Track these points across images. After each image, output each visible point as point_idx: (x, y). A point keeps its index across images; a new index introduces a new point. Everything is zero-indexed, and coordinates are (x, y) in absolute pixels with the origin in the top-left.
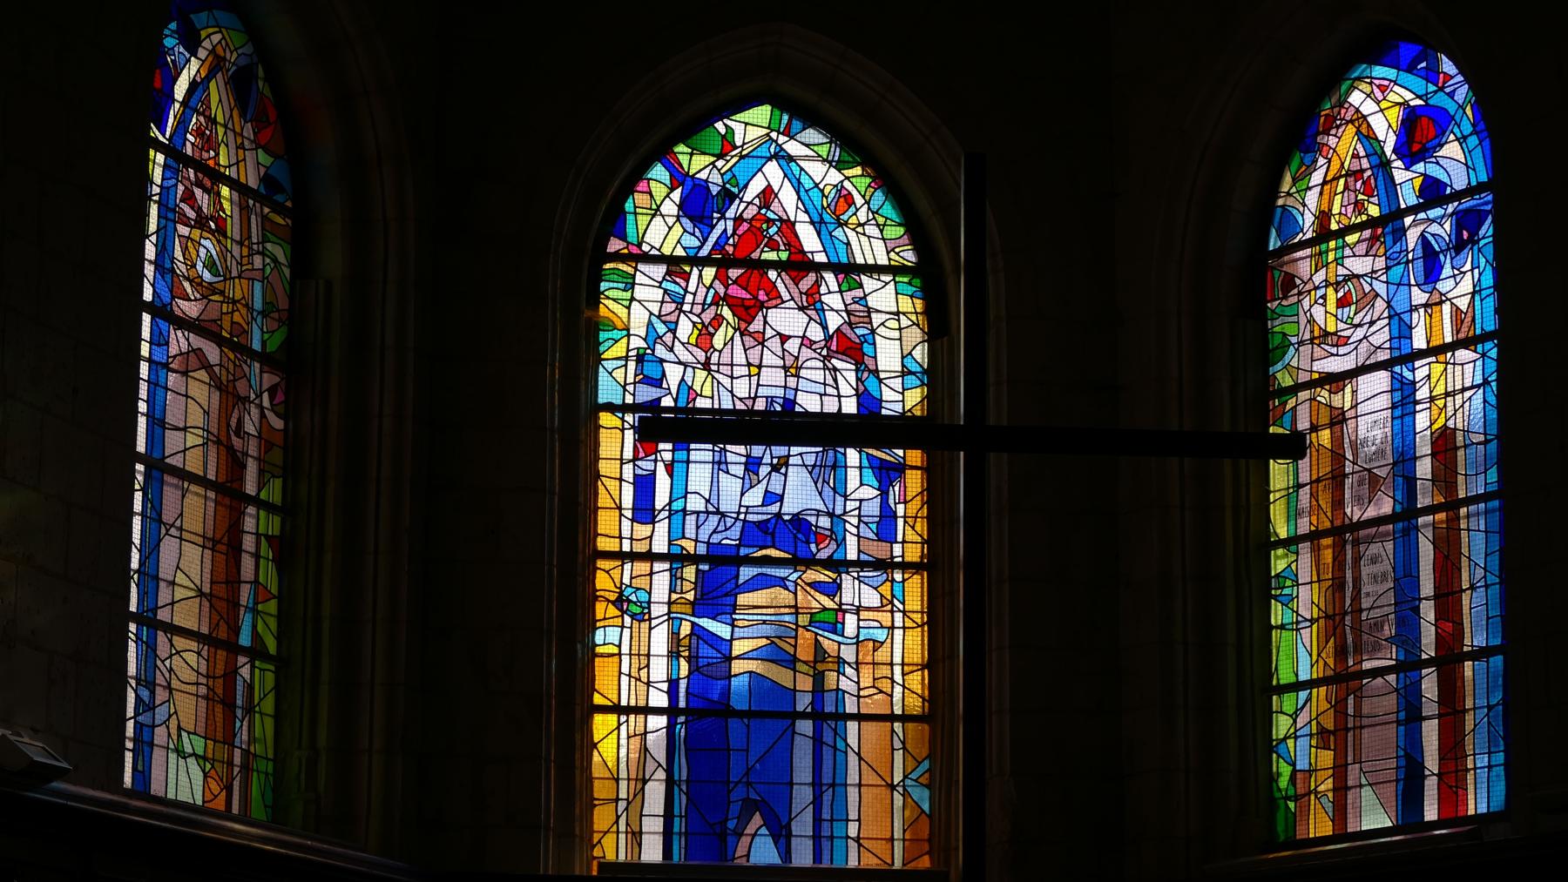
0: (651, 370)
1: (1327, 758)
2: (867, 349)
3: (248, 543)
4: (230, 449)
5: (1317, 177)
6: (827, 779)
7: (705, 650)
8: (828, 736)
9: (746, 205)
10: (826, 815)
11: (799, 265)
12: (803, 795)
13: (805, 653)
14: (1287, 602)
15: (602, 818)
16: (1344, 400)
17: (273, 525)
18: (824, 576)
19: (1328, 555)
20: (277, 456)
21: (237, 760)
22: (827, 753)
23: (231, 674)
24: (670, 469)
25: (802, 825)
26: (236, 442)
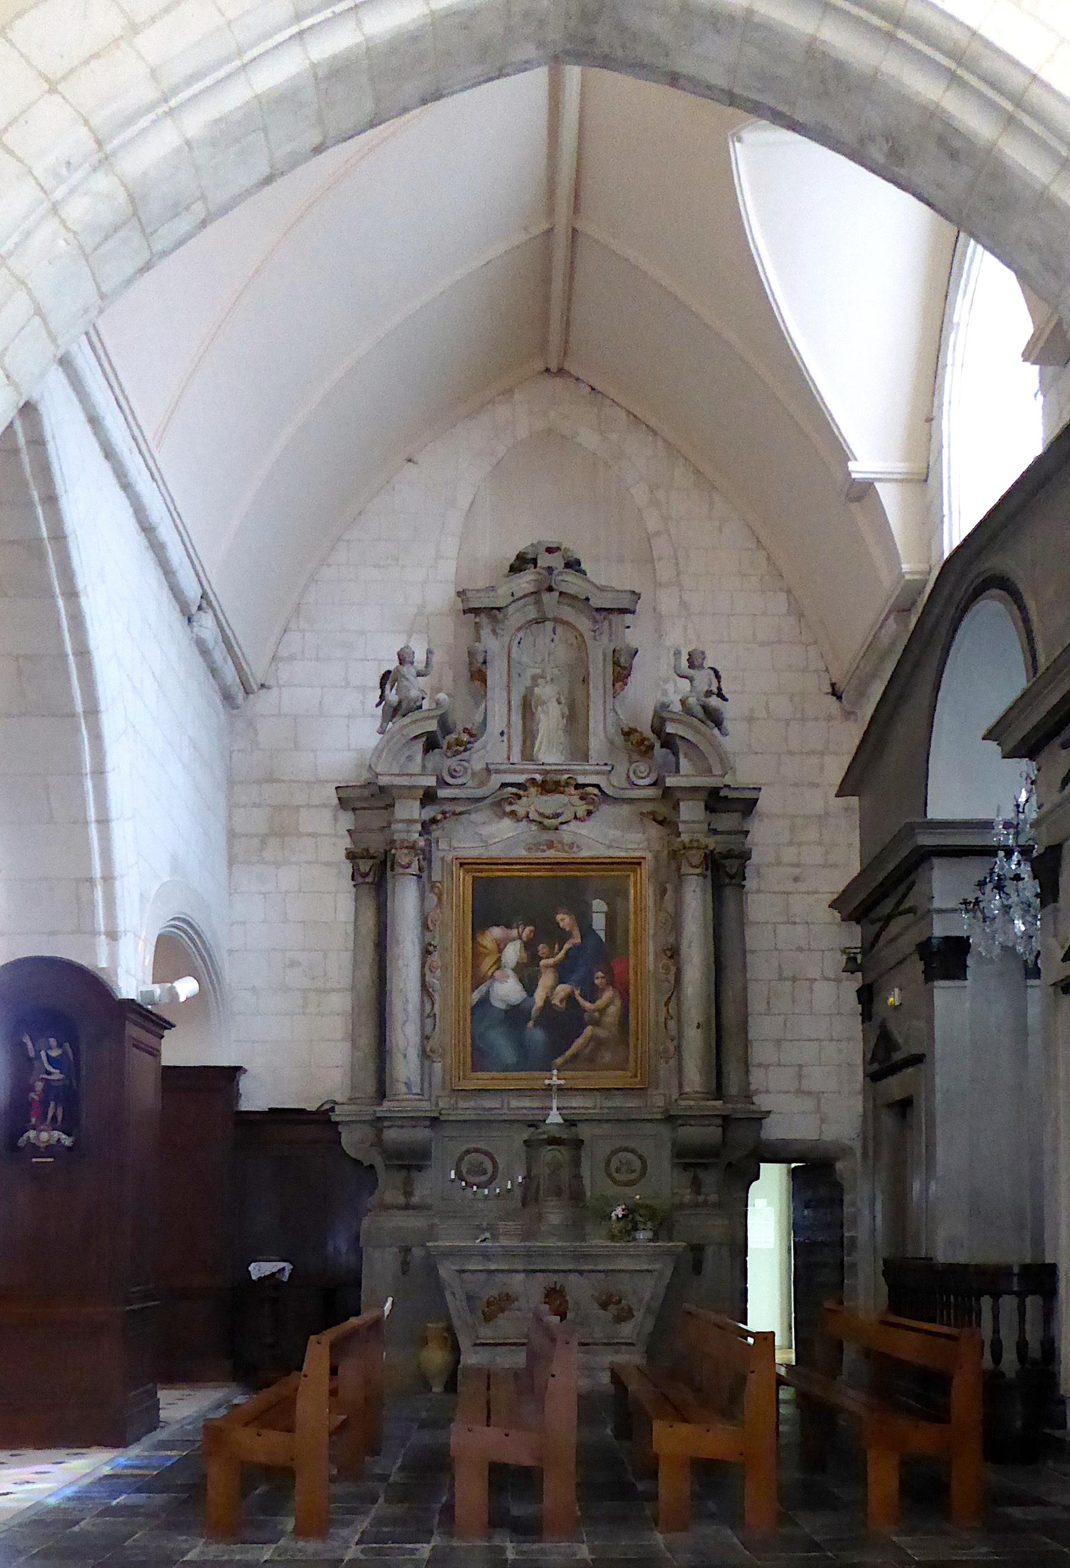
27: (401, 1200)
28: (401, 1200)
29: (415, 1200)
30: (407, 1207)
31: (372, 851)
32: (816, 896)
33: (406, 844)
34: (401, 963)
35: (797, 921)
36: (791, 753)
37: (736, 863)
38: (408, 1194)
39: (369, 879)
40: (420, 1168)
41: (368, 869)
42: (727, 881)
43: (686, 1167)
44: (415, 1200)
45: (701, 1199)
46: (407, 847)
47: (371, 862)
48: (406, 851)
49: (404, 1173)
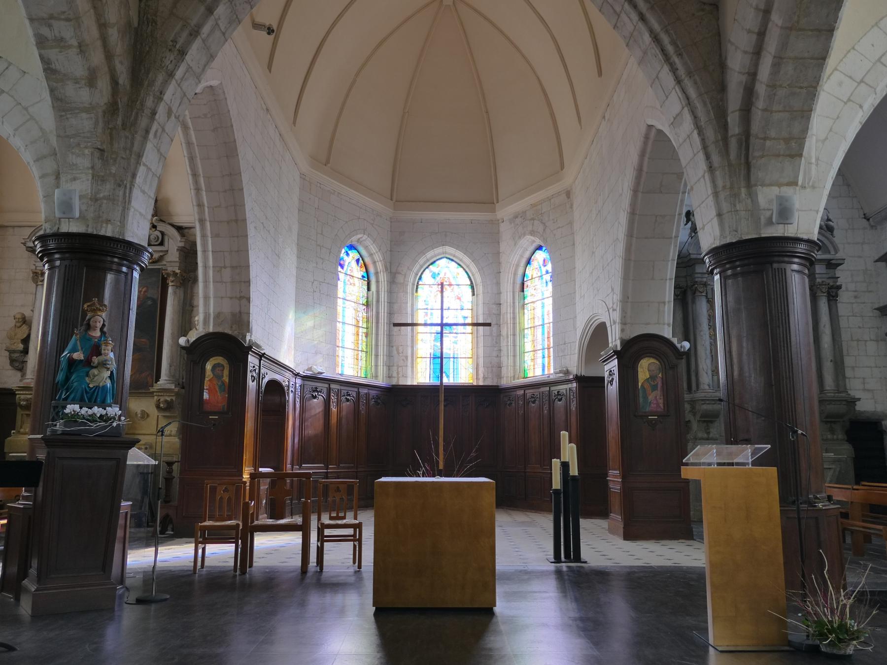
0: (427, 303)
1: (532, 364)
2: (461, 298)
3: (360, 334)
4: (357, 319)
5: (531, 269)
6: (455, 368)
7: (436, 348)
8: (455, 361)
9: (442, 275)
10: (455, 373)
11: (450, 285)
12: (451, 371)
13: (452, 348)
14: (527, 338)
15: (419, 375)
16: (534, 305)
17: (365, 330)
18: (455, 335)
19: (532, 331)
20: (365, 320)
21: (359, 368)
22: (455, 364)
23: (357, 355)
24: (430, 319)
25: (451, 376)
26: (358, 318)
27: (705, 436)
28: (705, 436)
29: (711, 435)
30: (708, 439)
31: (681, 285)
32: (865, 304)
33: (702, 283)
34: (702, 333)
35: (858, 315)
36: (849, 243)
37: (834, 290)
38: (708, 433)
39: (679, 297)
40: (712, 422)
41: (679, 293)
42: (832, 298)
43: (826, 422)
44: (711, 435)
45: (835, 437)
46: (702, 284)
47: (680, 290)
48: (702, 286)
49: (705, 424)
